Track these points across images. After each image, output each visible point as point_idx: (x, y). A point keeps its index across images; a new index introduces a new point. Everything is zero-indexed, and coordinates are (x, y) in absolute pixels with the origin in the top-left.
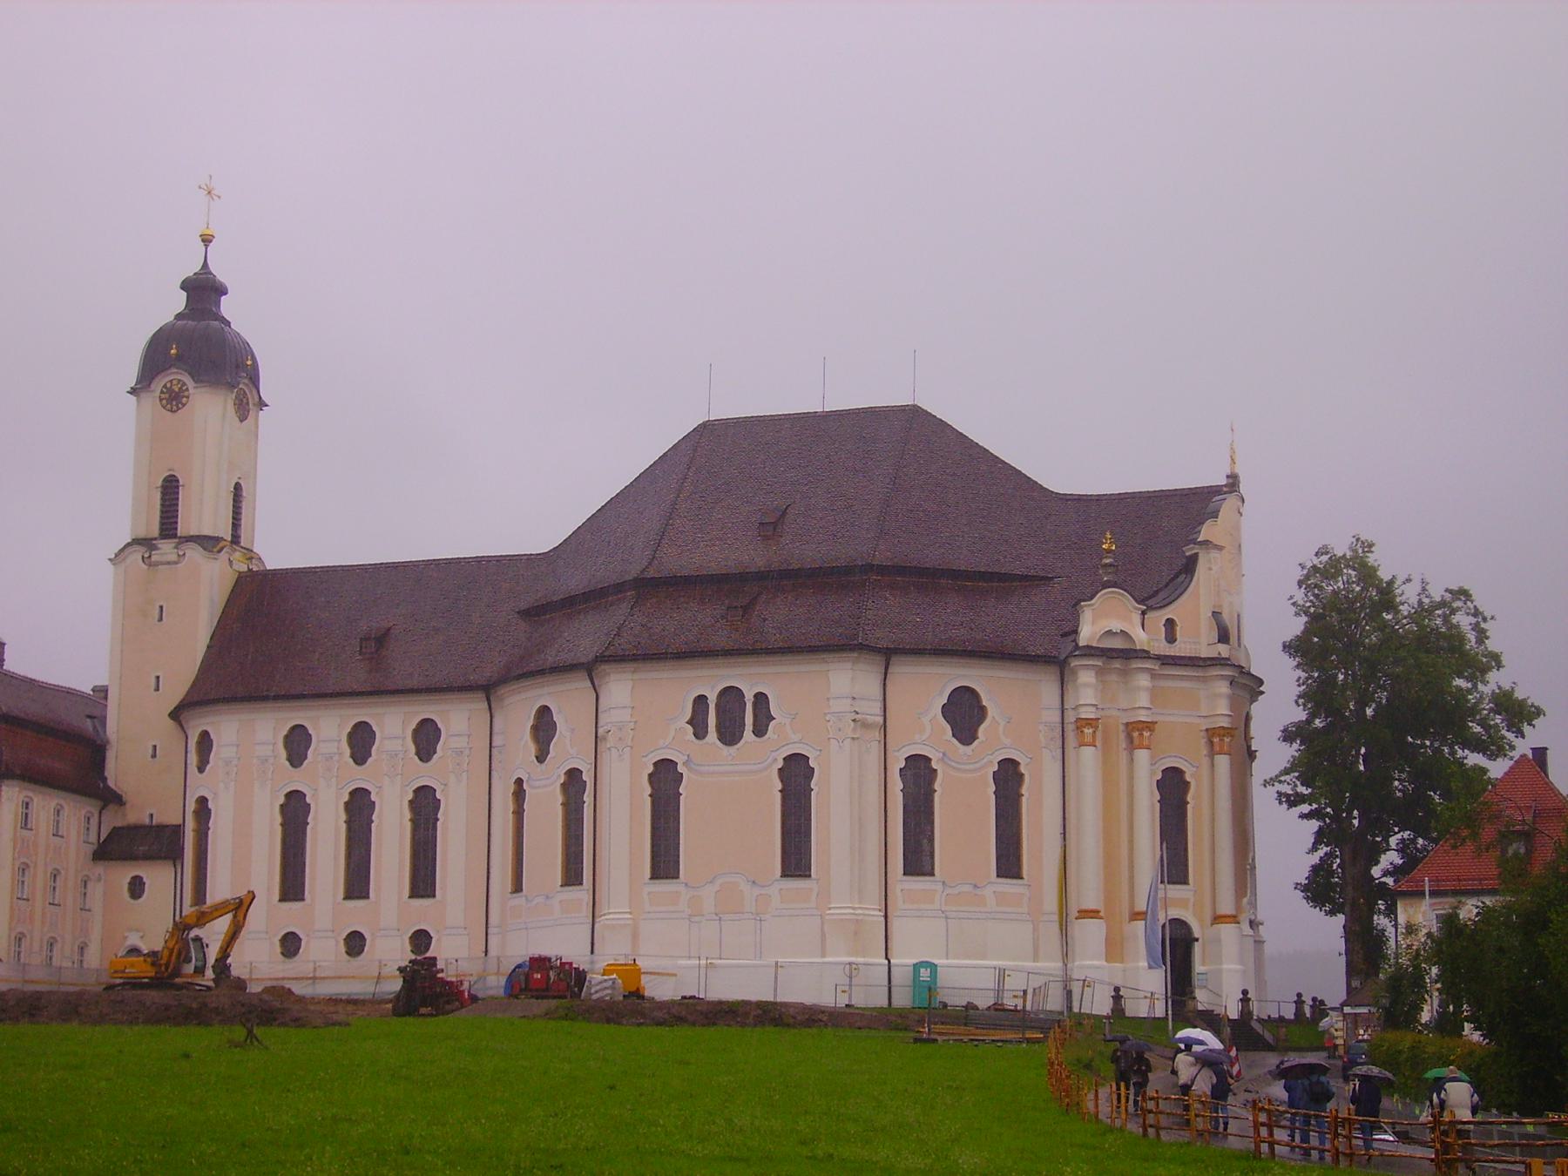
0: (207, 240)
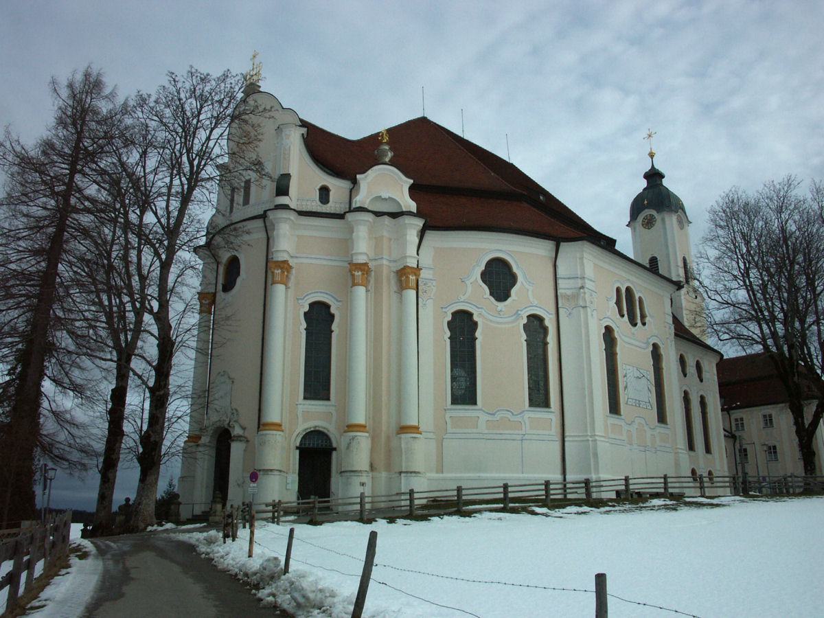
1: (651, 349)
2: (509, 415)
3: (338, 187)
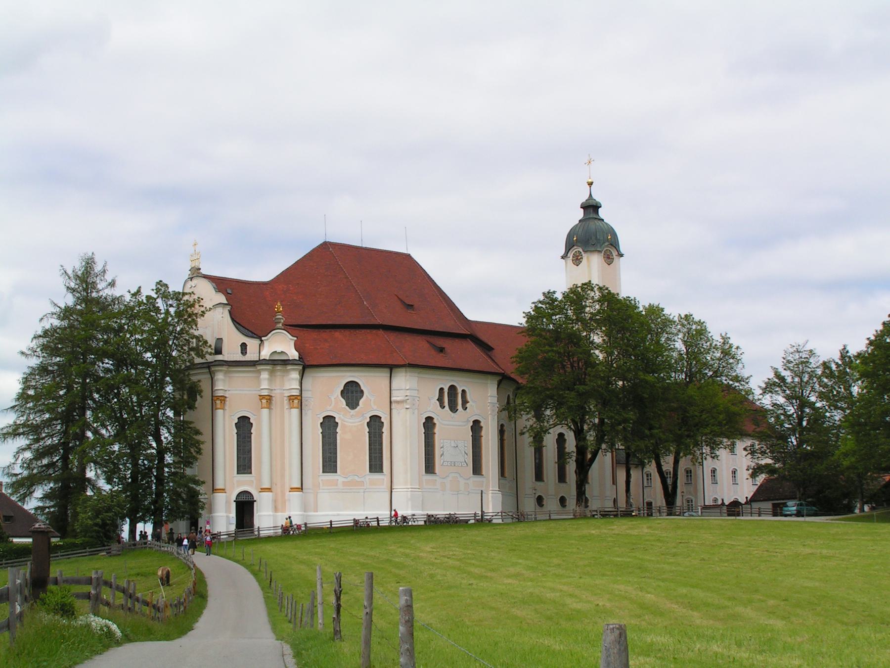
0: (590, 184)
1: (471, 424)
2: (356, 478)
3: (252, 344)
